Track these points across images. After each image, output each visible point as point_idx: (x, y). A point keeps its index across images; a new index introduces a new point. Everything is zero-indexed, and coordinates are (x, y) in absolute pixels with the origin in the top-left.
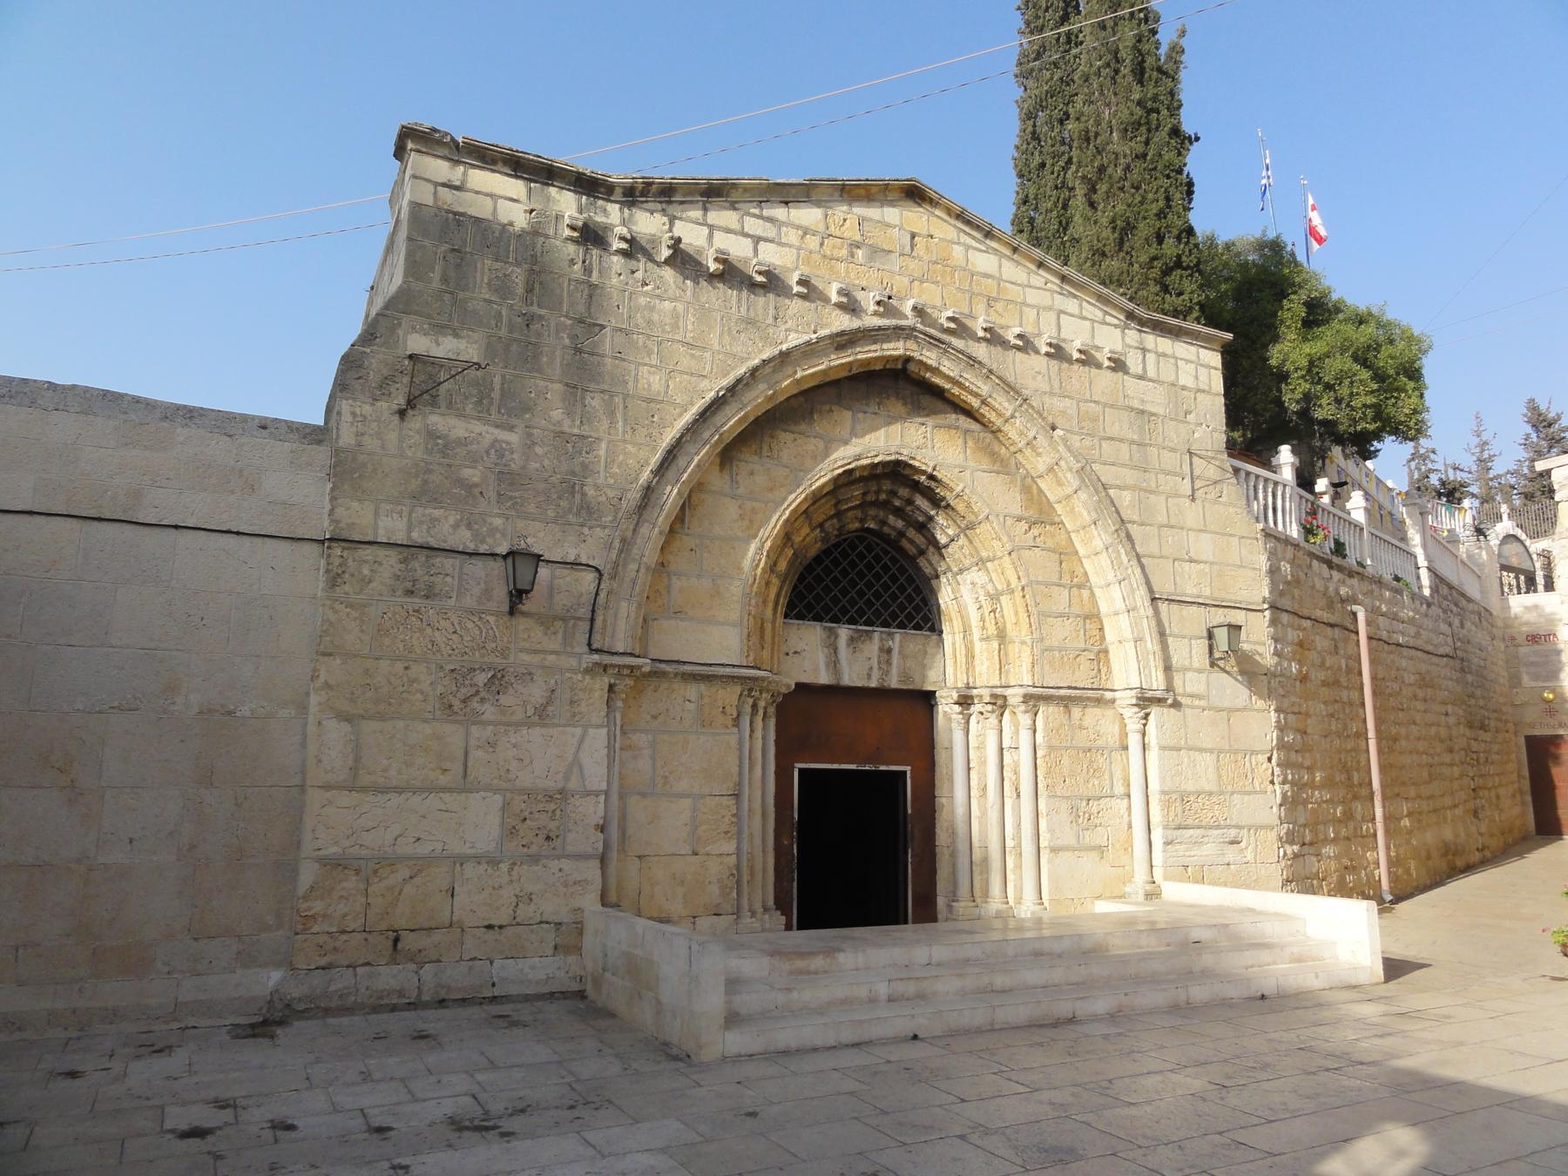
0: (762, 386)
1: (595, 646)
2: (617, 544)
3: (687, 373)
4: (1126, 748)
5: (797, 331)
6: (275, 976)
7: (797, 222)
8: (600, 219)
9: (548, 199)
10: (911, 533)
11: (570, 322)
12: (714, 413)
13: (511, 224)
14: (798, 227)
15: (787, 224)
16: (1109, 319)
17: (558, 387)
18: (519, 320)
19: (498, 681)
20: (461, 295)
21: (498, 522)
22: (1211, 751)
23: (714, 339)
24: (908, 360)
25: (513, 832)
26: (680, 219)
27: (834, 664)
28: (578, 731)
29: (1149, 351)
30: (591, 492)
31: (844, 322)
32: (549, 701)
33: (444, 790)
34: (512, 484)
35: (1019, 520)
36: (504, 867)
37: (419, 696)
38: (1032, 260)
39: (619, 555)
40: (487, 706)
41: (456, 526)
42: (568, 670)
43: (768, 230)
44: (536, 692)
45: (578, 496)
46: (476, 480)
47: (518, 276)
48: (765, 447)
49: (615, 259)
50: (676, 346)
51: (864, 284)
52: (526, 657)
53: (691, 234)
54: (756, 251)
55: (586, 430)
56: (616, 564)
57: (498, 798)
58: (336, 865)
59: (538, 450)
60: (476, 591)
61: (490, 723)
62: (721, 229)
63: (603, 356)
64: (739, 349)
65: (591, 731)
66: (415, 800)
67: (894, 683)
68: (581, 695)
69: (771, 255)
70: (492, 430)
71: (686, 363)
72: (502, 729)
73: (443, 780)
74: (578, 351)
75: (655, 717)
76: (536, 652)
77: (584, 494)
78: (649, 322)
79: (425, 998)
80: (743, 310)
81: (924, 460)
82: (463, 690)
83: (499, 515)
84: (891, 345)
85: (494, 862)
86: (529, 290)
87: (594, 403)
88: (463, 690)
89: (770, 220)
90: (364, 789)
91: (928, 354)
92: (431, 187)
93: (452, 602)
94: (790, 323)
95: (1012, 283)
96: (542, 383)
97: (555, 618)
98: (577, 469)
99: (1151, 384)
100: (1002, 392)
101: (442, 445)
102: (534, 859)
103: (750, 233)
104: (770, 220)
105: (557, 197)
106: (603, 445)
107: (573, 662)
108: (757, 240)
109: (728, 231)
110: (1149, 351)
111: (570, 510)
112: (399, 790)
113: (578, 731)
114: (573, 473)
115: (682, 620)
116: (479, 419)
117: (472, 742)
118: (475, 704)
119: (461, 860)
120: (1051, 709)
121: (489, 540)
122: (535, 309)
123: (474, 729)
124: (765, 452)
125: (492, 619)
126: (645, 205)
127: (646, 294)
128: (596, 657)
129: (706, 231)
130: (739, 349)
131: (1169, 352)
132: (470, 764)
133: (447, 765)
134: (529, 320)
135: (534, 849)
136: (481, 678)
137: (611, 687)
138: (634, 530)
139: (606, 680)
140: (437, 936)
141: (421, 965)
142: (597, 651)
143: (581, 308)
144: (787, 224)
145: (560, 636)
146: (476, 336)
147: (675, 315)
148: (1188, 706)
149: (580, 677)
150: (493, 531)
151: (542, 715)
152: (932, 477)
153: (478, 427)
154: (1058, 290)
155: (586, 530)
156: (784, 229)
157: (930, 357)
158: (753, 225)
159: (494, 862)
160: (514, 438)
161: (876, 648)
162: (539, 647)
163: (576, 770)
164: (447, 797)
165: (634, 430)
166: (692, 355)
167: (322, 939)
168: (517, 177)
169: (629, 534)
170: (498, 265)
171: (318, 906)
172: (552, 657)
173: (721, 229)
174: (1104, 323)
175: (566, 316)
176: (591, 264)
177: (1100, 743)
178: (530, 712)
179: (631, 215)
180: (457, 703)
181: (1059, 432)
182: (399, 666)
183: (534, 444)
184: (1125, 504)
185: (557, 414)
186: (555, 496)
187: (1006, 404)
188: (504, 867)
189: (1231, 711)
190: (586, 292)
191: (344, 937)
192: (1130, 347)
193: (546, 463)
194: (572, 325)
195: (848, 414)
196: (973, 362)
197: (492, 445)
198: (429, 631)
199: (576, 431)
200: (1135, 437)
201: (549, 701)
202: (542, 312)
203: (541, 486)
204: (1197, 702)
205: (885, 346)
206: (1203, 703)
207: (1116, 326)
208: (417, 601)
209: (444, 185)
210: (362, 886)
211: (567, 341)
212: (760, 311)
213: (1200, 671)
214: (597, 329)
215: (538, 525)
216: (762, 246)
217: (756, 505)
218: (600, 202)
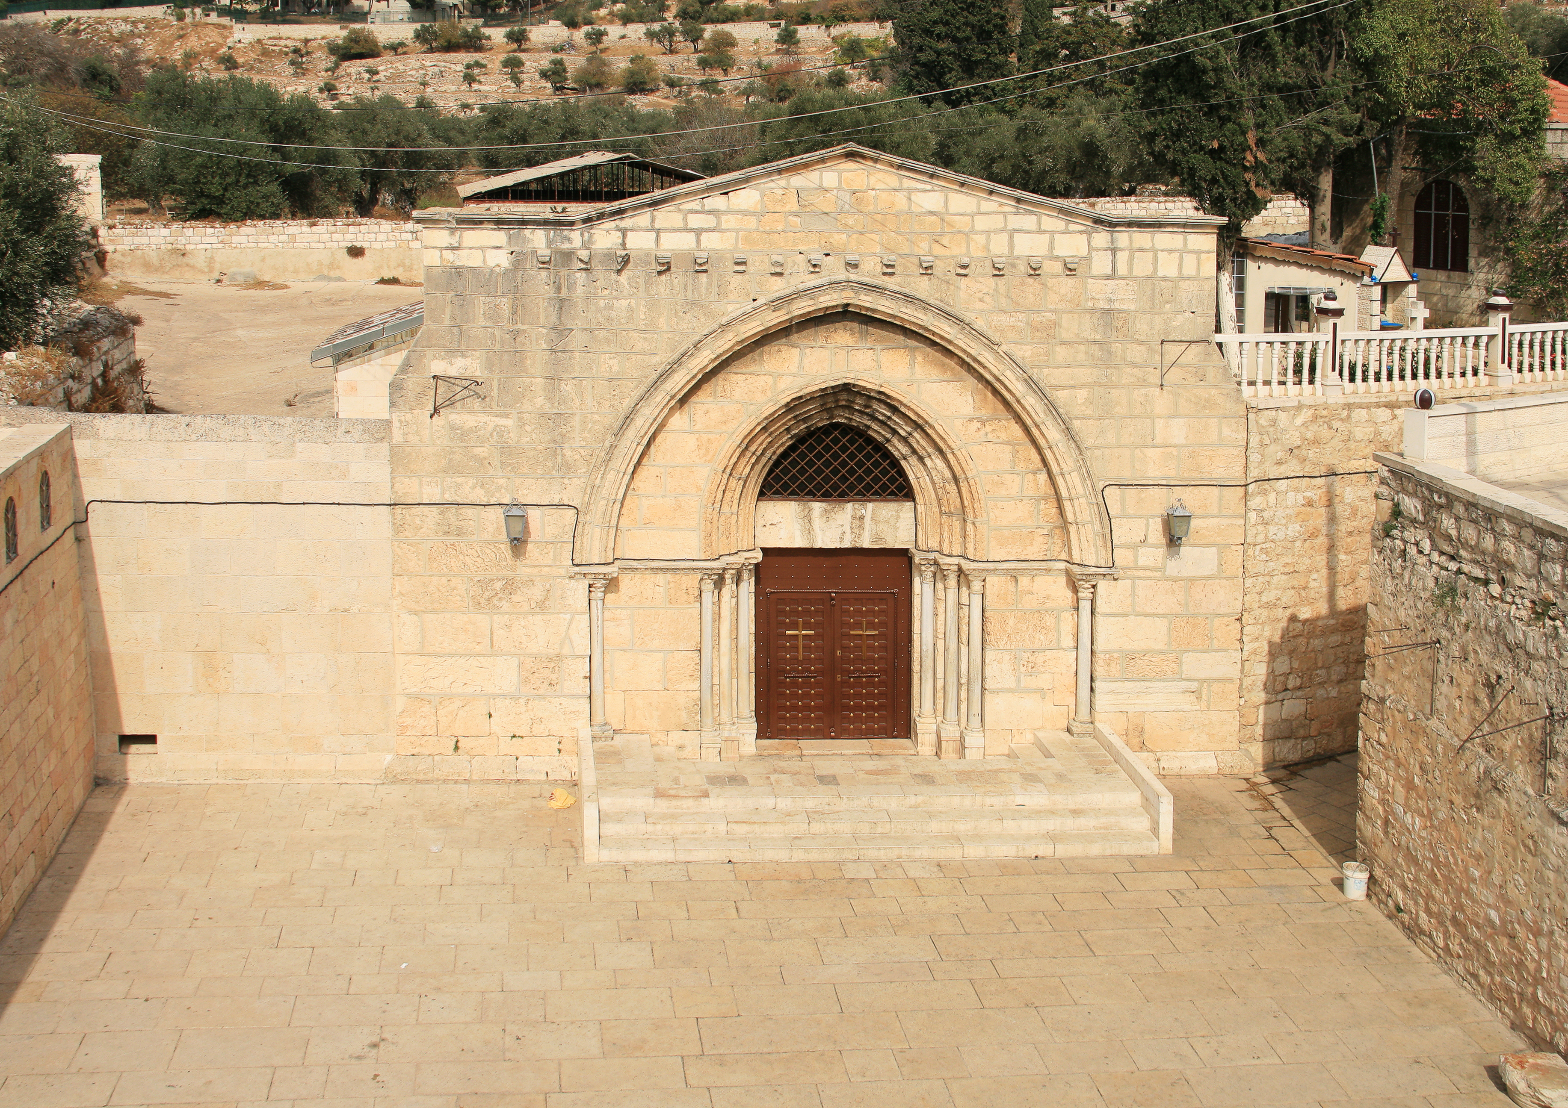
0: (705, 353)
1: (577, 562)
2: (589, 491)
3: (640, 354)
5: (737, 303)
6: (389, 757)
7: (736, 208)
8: (566, 246)
9: (525, 240)
11: (544, 331)
12: (663, 382)
13: (498, 265)
14: (738, 212)
15: (725, 213)
16: (1072, 227)
17: (539, 380)
18: (508, 336)
19: (510, 586)
20: (465, 327)
21: (502, 481)
22: (1164, 616)
23: (662, 322)
24: (848, 305)
25: (527, 681)
26: (632, 230)
28: (568, 616)
29: (1121, 250)
30: (568, 453)
31: (778, 287)
32: (547, 598)
33: (479, 655)
34: (510, 455)
35: (971, 420)
36: (522, 701)
37: (458, 598)
38: (983, 190)
39: (590, 498)
40: (504, 602)
41: (474, 488)
42: (559, 577)
43: (709, 221)
44: (537, 592)
45: (559, 458)
46: (486, 455)
47: (505, 304)
48: (719, 389)
49: (578, 275)
50: (631, 334)
51: (802, 248)
52: (529, 570)
54: (698, 241)
55: (562, 409)
56: (589, 503)
57: (514, 662)
58: (417, 697)
59: (527, 428)
60: (491, 529)
61: (507, 613)
62: (666, 230)
63: (572, 352)
64: (685, 326)
65: (577, 617)
66: (462, 661)
68: (569, 593)
69: (711, 241)
70: (494, 419)
71: (640, 345)
72: (514, 616)
73: (478, 648)
74: (553, 351)
75: (630, 598)
76: (534, 566)
77: (563, 455)
78: (609, 319)
79: (475, 777)
80: (689, 292)
82: (487, 593)
83: (502, 477)
84: (828, 297)
85: (514, 698)
86: (515, 313)
87: (567, 388)
88: (487, 593)
89: (710, 212)
90: (429, 655)
91: (865, 298)
92: (438, 252)
93: (475, 537)
94: (732, 297)
95: (961, 214)
96: (528, 380)
97: (547, 543)
98: (558, 438)
99: (1123, 282)
100: (943, 320)
101: (461, 434)
102: (542, 697)
103: (695, 227)
105: (531, 237)
106: (577, 418)
107: (563, 572)
108: (698, 232)
109: (675, 230)
110: (1121, 250)
111: (553, 467)
112: (451, 655)
113: (568, 616)
114: (555, 441)
115: (651, 529)
116: (485, 412)
117: (495, 626)
118: (495, 601)
119: (494, 696)
120: (996, 579)
121: (497, 495)
122: (519, 326)
123: (495, 617)
124: (719, 394)
125: (502, 546)
126: (602, 226)
127: (604, 298)
128: (577, 569)
129: (654, 234)
130: (685, 326)
131: (1148, 245)
132: (495, 639)
133: (479, 640)
134: (515, 334)
135: (541, 691)
136: (498, 585)
137: (590, 586)
138: (602, 478)
139: (587, 583)
140: (482, 741)
141: (473, 757)
142: (578, 565)
143: (554, 319)
145: (551, 554)
146: (477, 354)
147: (630, 310)
148: (1139, 578)
149: (567, 581)
150: (499, 488)
151: (542, 606)
153: (483, 418)
154: (1014, 210)
155: (566, 481)
156: (724, 218)
157: (866, 301)
158: (695, 221)
159: (514, 698)
160: (509, 422)
161: (849, 516)
162: (537, 563)
163: (567, 641)
164: (481, 659)
165: (599, 403)
166: (645, 339)
167: (413, 739)
168: (500, 229)
169: (598, 481)
170: (489, 299)
171: (408, 721)
172: (546, 569)
173: (666, 230)
174: (1066, 232)
175: (543, 327)
176: (560, 284)
177: (1048, 605)
178: (533, 605)
179: (591, 236)
180: (483, 601)
181: (1004, 347)
182: (444, 580)
183: (524, 424)
184: (1079, 402)
185: (540, 401)
186: (541, 459)
187: (948, 329)
188: (522, 701)
189: (1192, 580)
190: (557, 306)
191: (426, 738)
192: (1098, 249)
193: (534, 436)
194: (548, 334)
195: (796, 351)
196: (909, 299)
197: (494, 430)
198: (461, 557)
199: (555, 411)
200: (1098, 337)
201: (547, 598)
202: (525, 327)
203: (531, 454)
204: (1149, 573)
205: (822, 299)
206: (1158, 574)
207: (1081, 232)
208: (452, 539)
209: (447, 249)
210: (433, 711)
211: (544, 346)
212: (704, 291)
213: (1156, 547)
214: (567, 332)
215: (531, 481)
216: (704, 236)
217: (710, 436)
218: (566, 233)
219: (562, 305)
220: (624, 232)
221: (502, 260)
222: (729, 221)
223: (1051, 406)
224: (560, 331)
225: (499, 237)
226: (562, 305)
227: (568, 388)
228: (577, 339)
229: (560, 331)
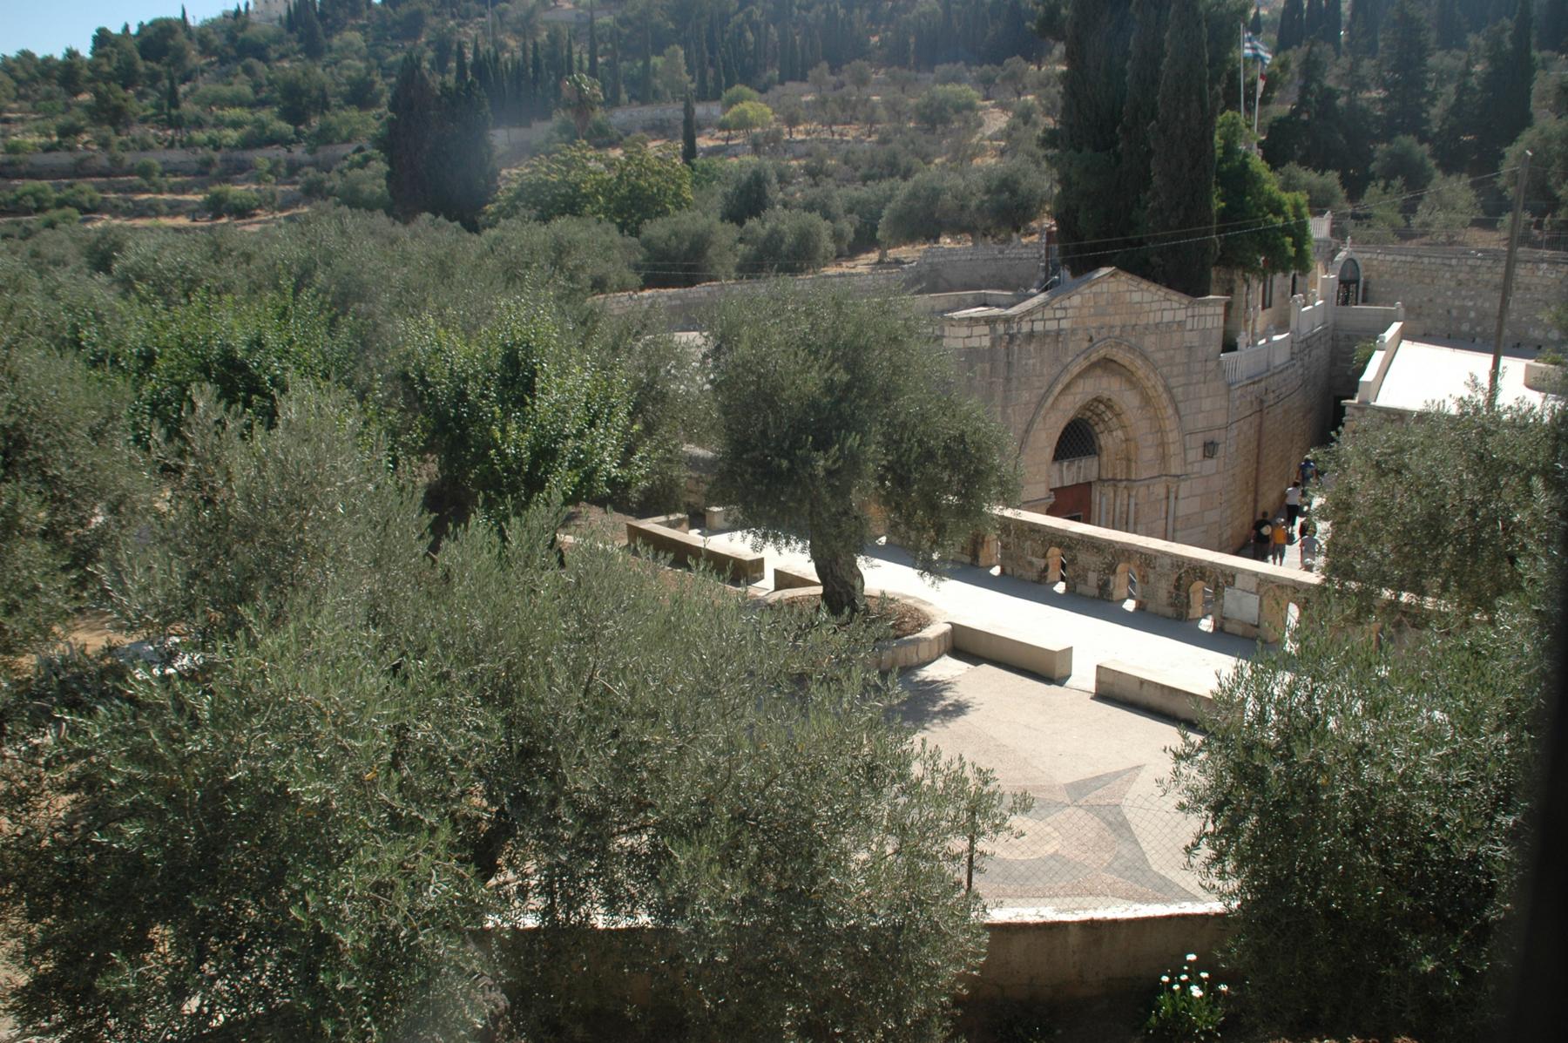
4: (1168, 498)
10: (1095, 417)
27: (1061, 478)
47: (987, 366)
53: (1038, 326)
67: (1081, 481)
81: (1106, 395)
104: (1065, 309)
108: (1059, 319)
134: (991, 383)
144: (1071, 307)
147: (1034, 365)
152: (1109, 400)
158: (1059, 314)
219: (1009, 364)
220: (1033, 321)
221: (986, 342)
222: (1070, 312)
223: (1172, 399)
224: (1008, 380)
225: (986, 330)
226: (1009, 364)
227: (1009, 411)
228: (1014, 383)
229: (1008, 380)
